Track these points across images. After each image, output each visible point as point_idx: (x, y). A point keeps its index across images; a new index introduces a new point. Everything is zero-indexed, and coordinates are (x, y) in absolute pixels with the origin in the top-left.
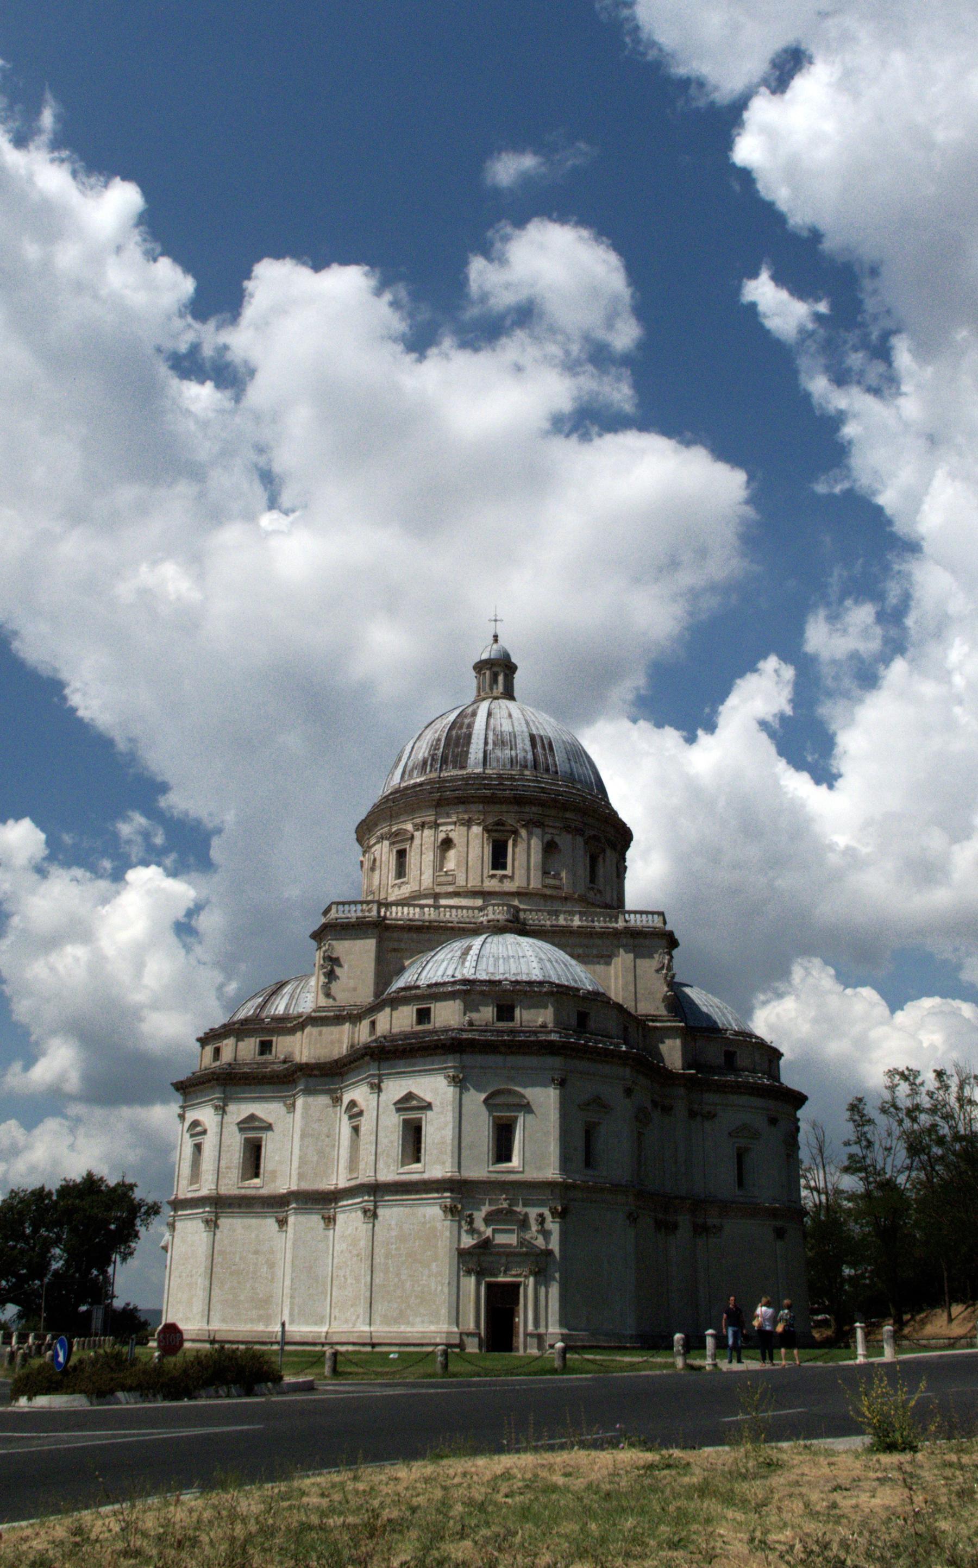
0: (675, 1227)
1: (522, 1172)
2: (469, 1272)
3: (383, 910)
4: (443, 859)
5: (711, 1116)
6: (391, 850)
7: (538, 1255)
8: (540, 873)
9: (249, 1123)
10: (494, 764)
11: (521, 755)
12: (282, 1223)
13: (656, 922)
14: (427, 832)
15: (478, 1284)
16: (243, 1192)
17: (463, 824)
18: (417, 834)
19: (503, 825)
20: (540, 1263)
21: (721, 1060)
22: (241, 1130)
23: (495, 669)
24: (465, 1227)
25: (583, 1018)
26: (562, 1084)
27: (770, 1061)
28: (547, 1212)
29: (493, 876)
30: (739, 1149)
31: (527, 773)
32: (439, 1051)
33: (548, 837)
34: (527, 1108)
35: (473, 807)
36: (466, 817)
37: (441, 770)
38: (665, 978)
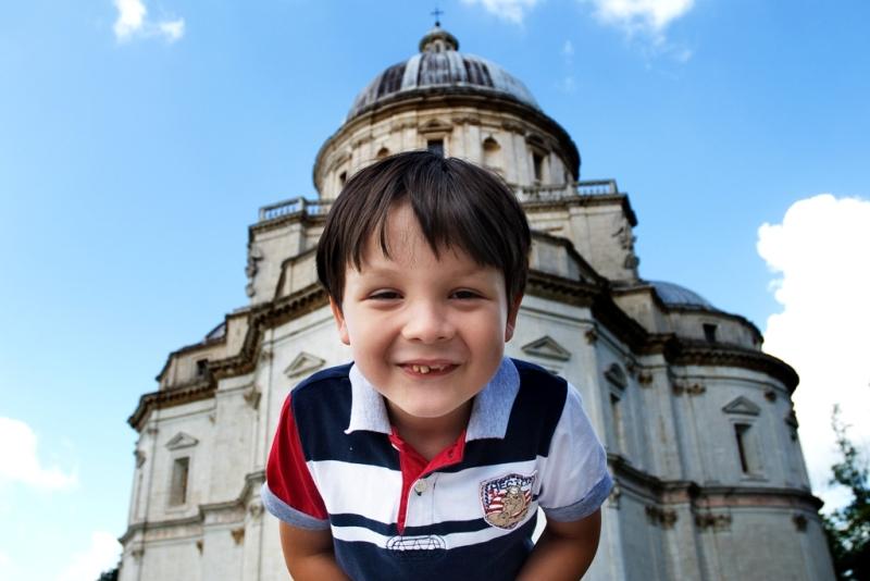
0: (674, 518)
5: (698, 391)
6: (334, 179)
9: (177, 442)
10: (427, 80)
11: (454, 72)
12: (200, 546)
13: (608, 189)
14: (365, 148)
16: (170, 517)
18: (356, 153)
21: (700, 334)
23: (437, 42)
27: (755, 342)
31: (461, 84)
33: (485, 136)
37: (379, 96)
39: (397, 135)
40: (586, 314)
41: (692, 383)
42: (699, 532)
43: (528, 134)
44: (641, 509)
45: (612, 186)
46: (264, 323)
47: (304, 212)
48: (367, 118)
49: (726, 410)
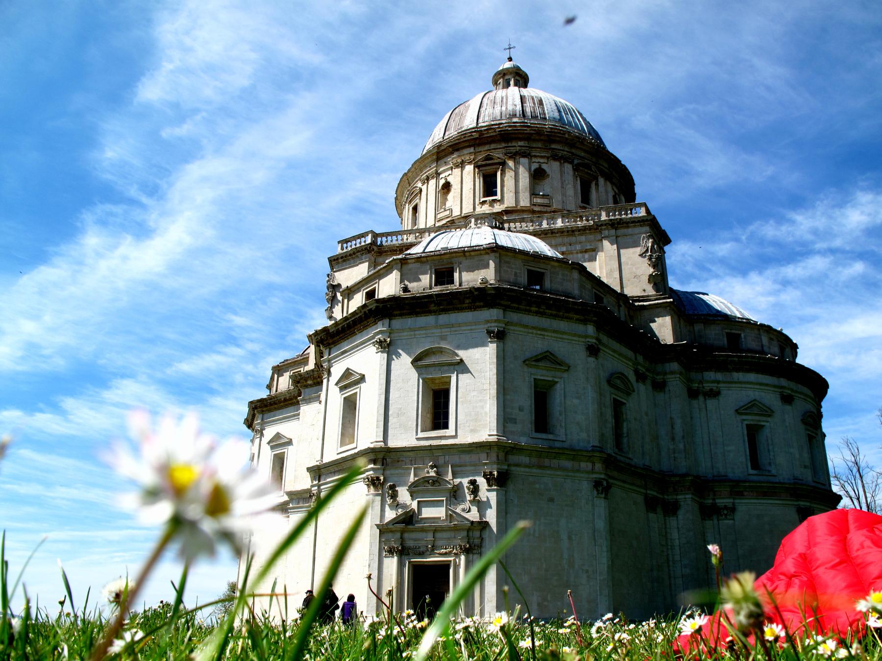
1: (455, 437)
2: (391, 552)
3: (379, 239)
4: (445, 200)
5: (714, 394)
7: (468, 530)
8: (527, 194)
11: (510, 108)
14: (432, 182)
15: (401, 566)
17: (457, 167)
19: (492, 159)
20: (473, 540)
21: (725, 341)
22: (272, 448)
23: (507, 77)
24: (389, 501)
25: (535, 277)
26: (499, 336)
28: (481, 481)
29: (484, 203)
30: (748, 426)
32: (372, 319)
33: (535, 166)
34: (461, 367)
35: (466, 151)
36: (459, 160)
38: (650, 259)
39: (457, 171)
40: (591, 329)
41: (707, 386)
42: (703, 519)
43: (576, 162)
44: (640, 499)
45: (643, 210)
46: (323, 344)
47: (374, 243)
48: (433, 154)
49: (736, 411)
